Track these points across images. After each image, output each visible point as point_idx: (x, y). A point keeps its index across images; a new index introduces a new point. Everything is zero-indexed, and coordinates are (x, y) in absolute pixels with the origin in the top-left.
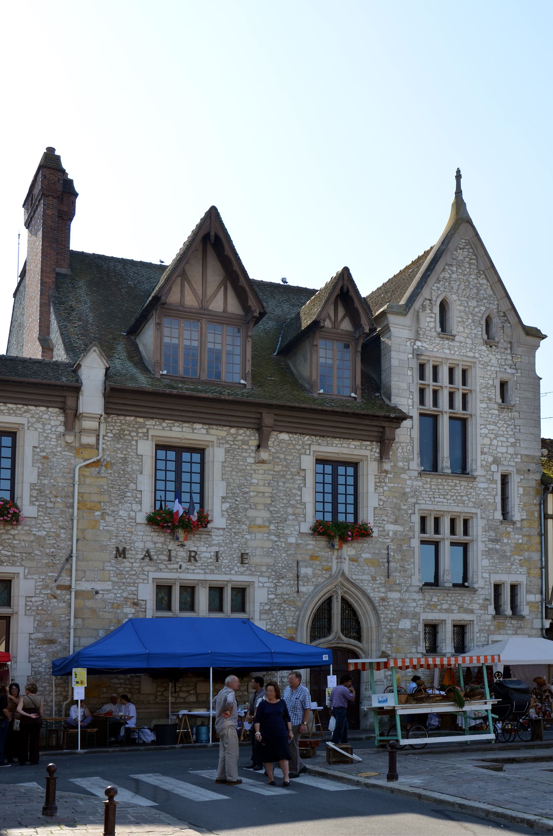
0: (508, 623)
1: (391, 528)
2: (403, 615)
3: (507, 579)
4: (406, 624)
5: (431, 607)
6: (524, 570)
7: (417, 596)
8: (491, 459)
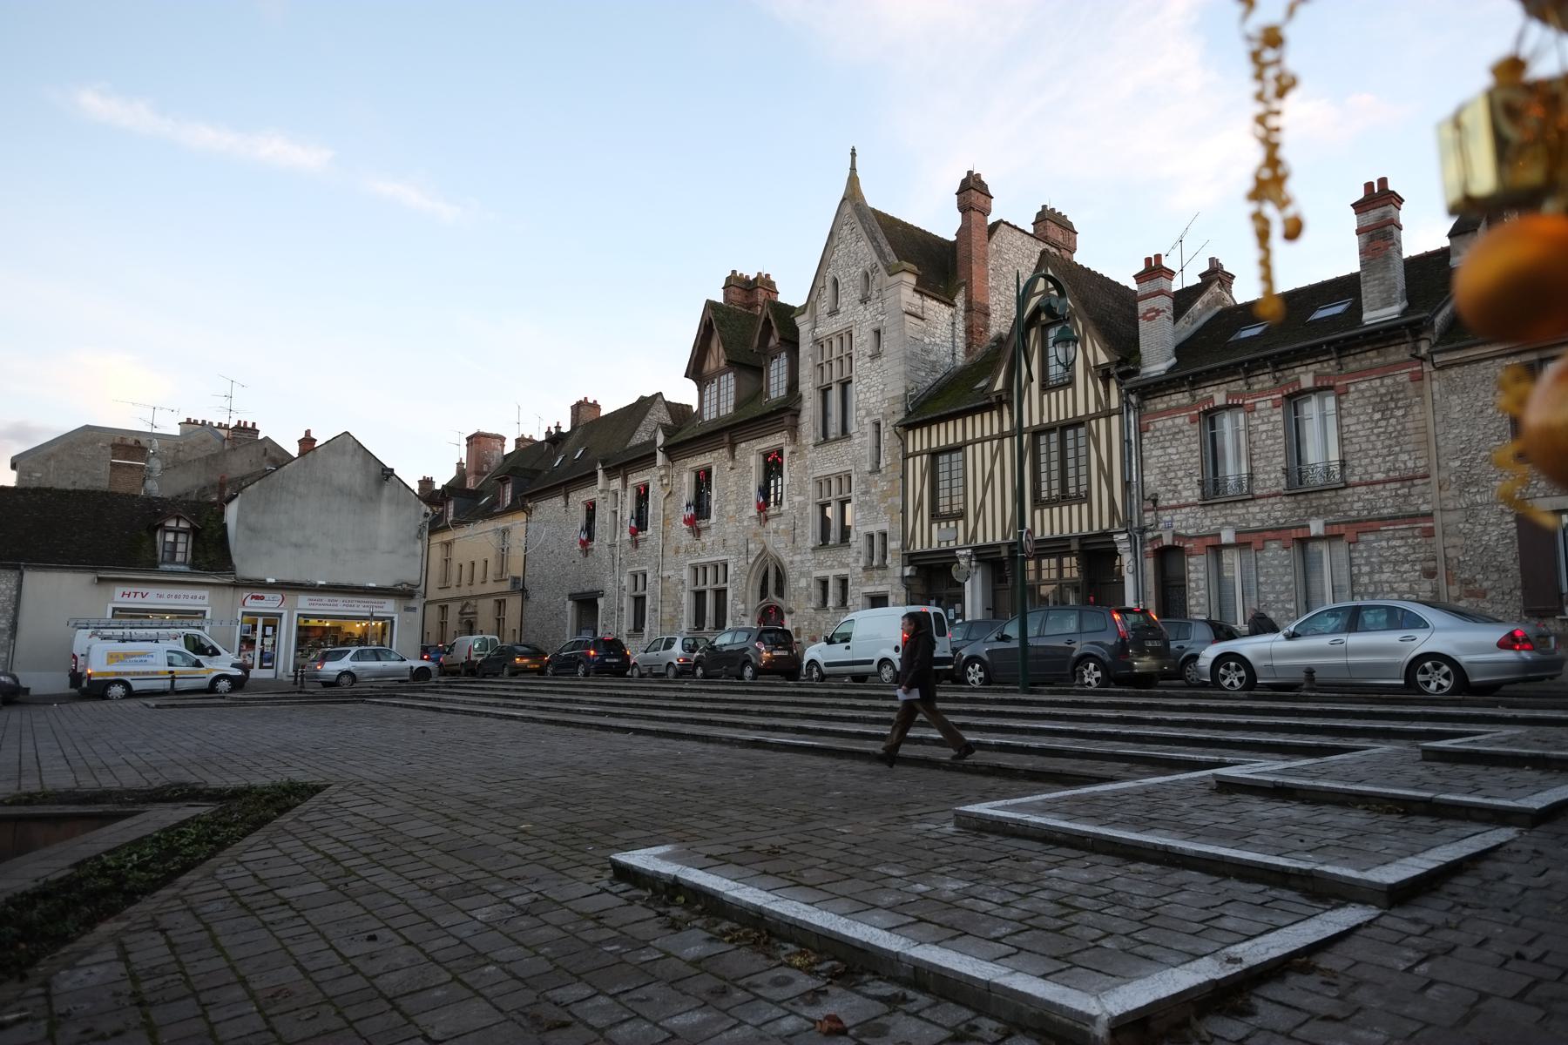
0: (876, 574)
1: (797, 499)
2: (802, 574)
3: (874, 528)
4: (803, 583)
5: (820, 565)
6: (887, 517)
7: (810, 557)
8: (863, 413)
